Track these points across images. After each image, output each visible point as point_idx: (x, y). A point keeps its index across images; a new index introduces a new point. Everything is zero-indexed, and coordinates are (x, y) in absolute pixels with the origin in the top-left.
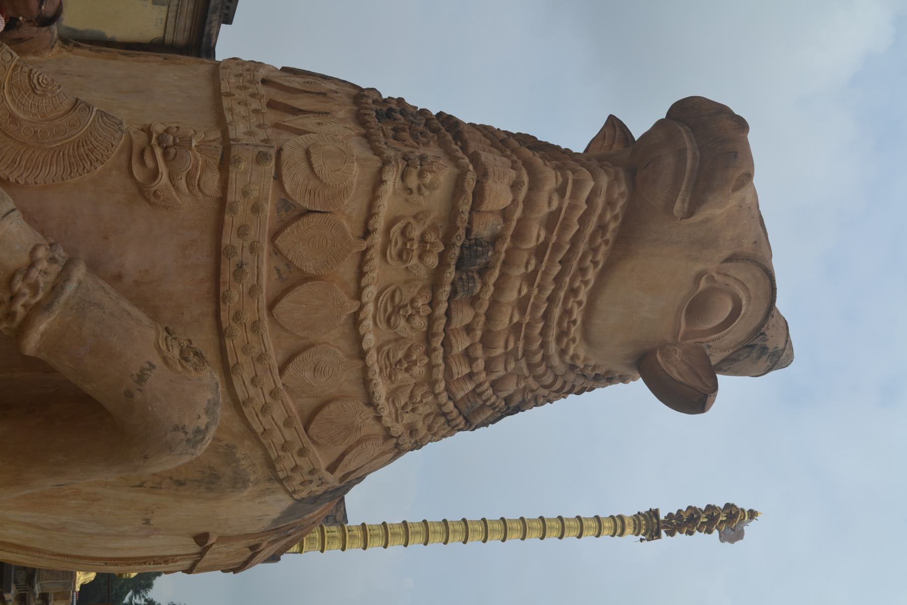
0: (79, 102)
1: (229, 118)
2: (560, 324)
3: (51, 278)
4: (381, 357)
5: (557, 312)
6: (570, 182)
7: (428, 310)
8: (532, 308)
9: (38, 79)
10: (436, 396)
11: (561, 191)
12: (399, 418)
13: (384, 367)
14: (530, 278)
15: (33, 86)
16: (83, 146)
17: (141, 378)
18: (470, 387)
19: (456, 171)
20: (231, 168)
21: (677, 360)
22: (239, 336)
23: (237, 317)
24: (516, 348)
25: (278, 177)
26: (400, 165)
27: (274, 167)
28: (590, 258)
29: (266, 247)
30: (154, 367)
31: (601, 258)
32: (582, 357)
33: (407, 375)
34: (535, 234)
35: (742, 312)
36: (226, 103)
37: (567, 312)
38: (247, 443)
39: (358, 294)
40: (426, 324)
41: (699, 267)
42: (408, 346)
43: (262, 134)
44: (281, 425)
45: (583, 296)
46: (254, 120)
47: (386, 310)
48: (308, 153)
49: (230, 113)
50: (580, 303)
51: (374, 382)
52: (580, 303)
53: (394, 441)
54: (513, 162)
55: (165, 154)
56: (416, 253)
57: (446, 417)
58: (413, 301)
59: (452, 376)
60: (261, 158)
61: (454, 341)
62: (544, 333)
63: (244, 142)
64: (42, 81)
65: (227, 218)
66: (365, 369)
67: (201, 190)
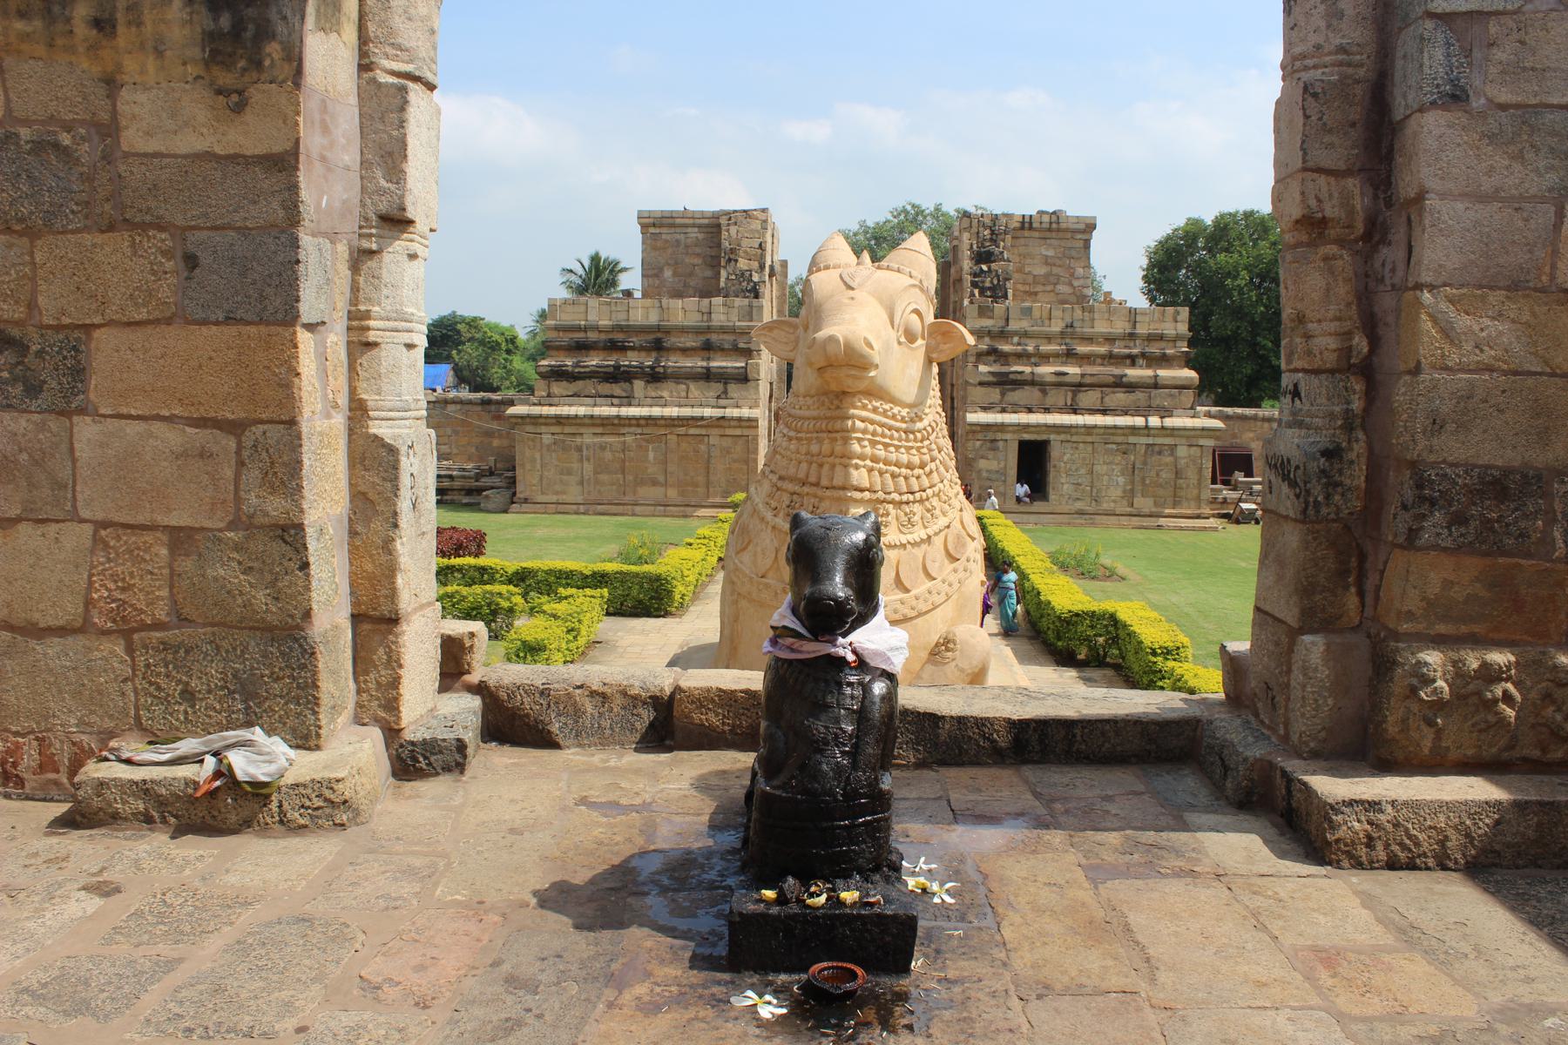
14: (897, 448)
17: (962, 670)
22: (923, 607)
34: (881, 453)
41: (896, 344)
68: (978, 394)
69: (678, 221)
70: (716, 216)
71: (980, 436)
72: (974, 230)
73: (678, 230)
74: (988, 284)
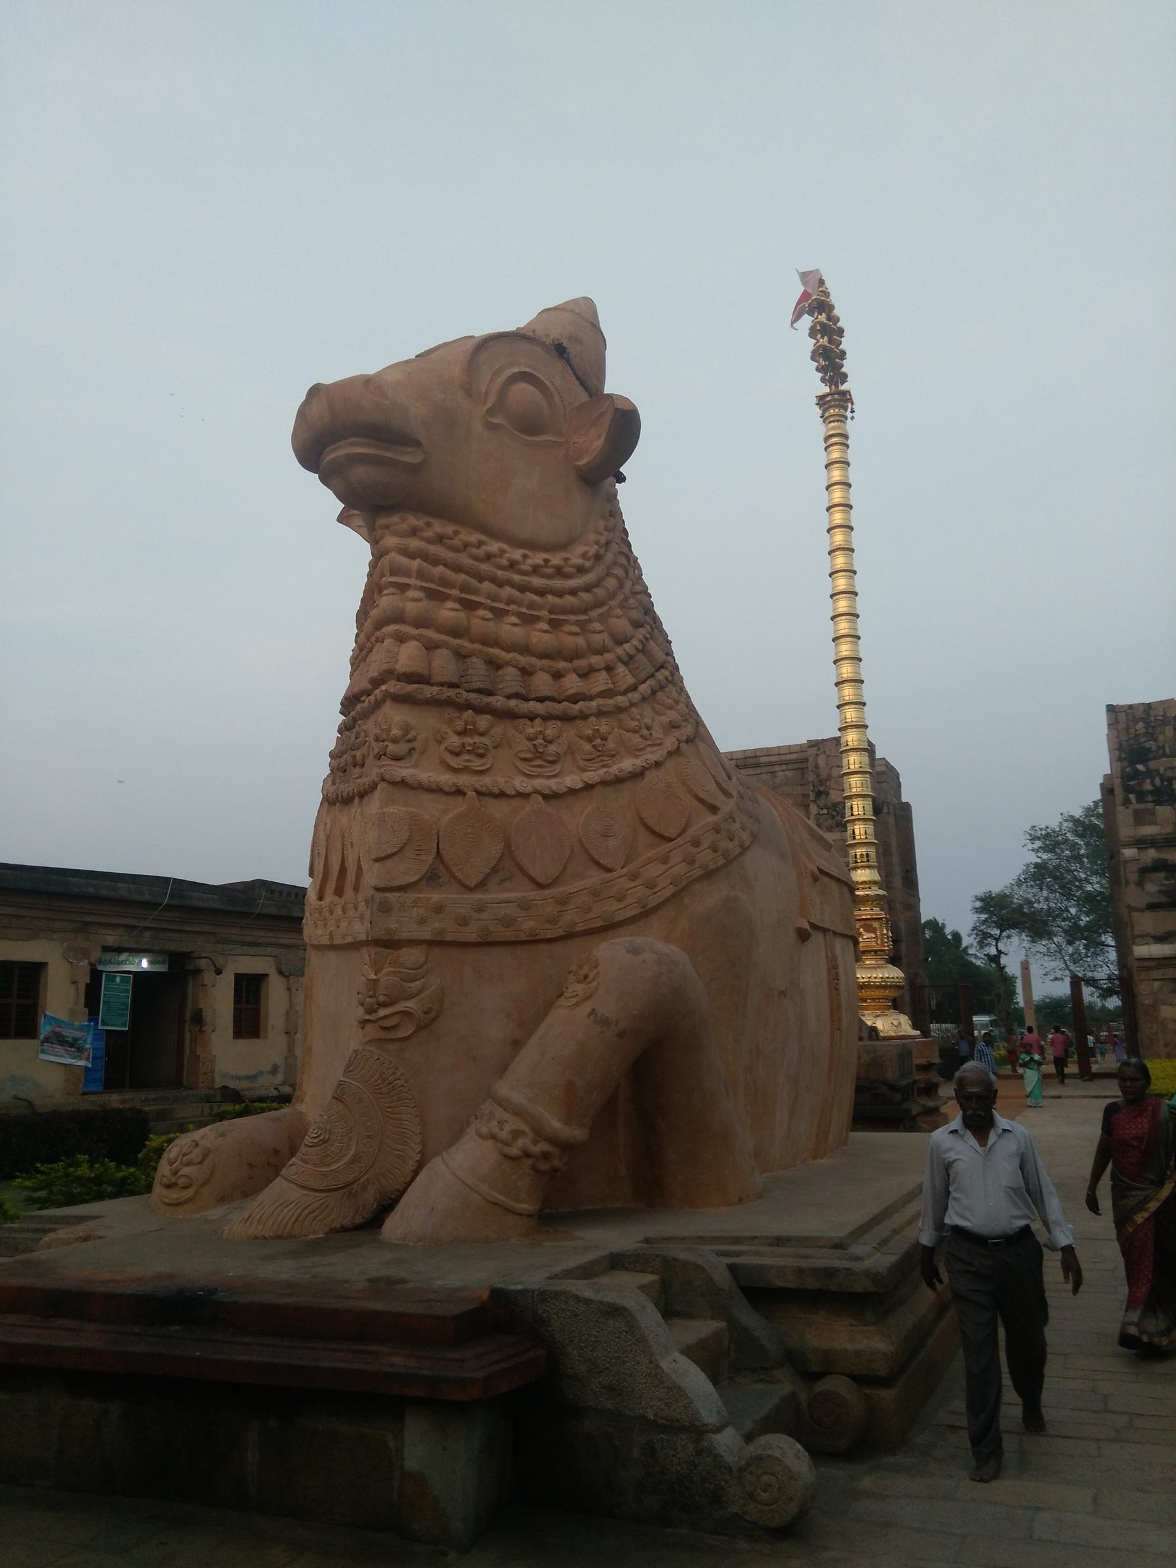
0: (335, 1095)
1: (349, 940)
2: (550, 577)
3: (506, 1116)
4: (590, 767)
5: (537, 581)
6: (393, 579)
7: (537, 721)
8: (534, 609)
9: (315, 1138)
10: (632, 705)
11: (403, 588)
12: (657, 742)
13: (602, 764)
14: (499, 614)
15: (321, 1142)
16: (379, 1089)
17: (605, 1023)
18: (621, 669)
19: (388, 703)
20: (397, 938)
21: (585, 441)
22: (571, 917)
23: (552, 921)
24: (577, 623)
25: (402, 888)
26: (384, 763)
27: (392, 894)
28: (474, 551)
29: (477, 896)
30: (593, 1010)
31: (474, 538)
32: (586, 549)
33: (611, 737)
34: (448, 612)
35: (528, 370)
36: (338, 941)
37: (536, 570)
38: (686, 901)
39: (525, 796)
40: (553, 722)
42: (578, 739)
43: (362, 907)
44: (666, 867)
45: (517, 554)
46: (351, 913)
47: (540, 766)
48: (377, 860)
49: (346, 937)
50: (525, 557)
51: (617, 773)
52: (525, 557)
53: (683, 745)
54: (377, 640)
55: (384, 1005)
56: (477, 739)
57: (657, 691)
58: (530, 739)
59: (609, 690)
60: (385, 908)
61: (571, 692)
62: (559, 594)
63: (369, 926)
64: (316, 1133)
65: (449, 938)
66: (604, 783)
67: (421, 967)
68: (1146, 922)
69: (763, 760)
70: (801, 749)
71: (1157, 974)
72: (1121, 726)
73: (764, 770)
74: (1148, 786)
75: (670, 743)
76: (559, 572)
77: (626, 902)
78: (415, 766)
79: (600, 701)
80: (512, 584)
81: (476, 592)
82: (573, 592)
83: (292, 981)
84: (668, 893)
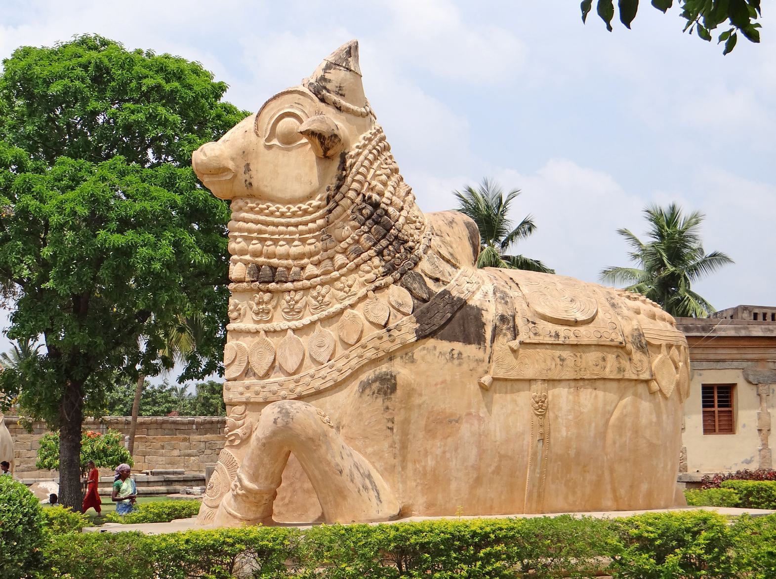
2: (302, 216)
5: (293, 220)
8: (292, 235)
14: (276, 242)
24: (313, 237)
37: (294, 214)
62: (306, 224)
75: (362, 292)
76: (306, 212)
77: (327, 379)
78: (241, 322)
79: (322, 277)
80: (282, 225)
81: (265, 232)
82: (314, 221)
83: (761, 388)
84: (348, 373)
